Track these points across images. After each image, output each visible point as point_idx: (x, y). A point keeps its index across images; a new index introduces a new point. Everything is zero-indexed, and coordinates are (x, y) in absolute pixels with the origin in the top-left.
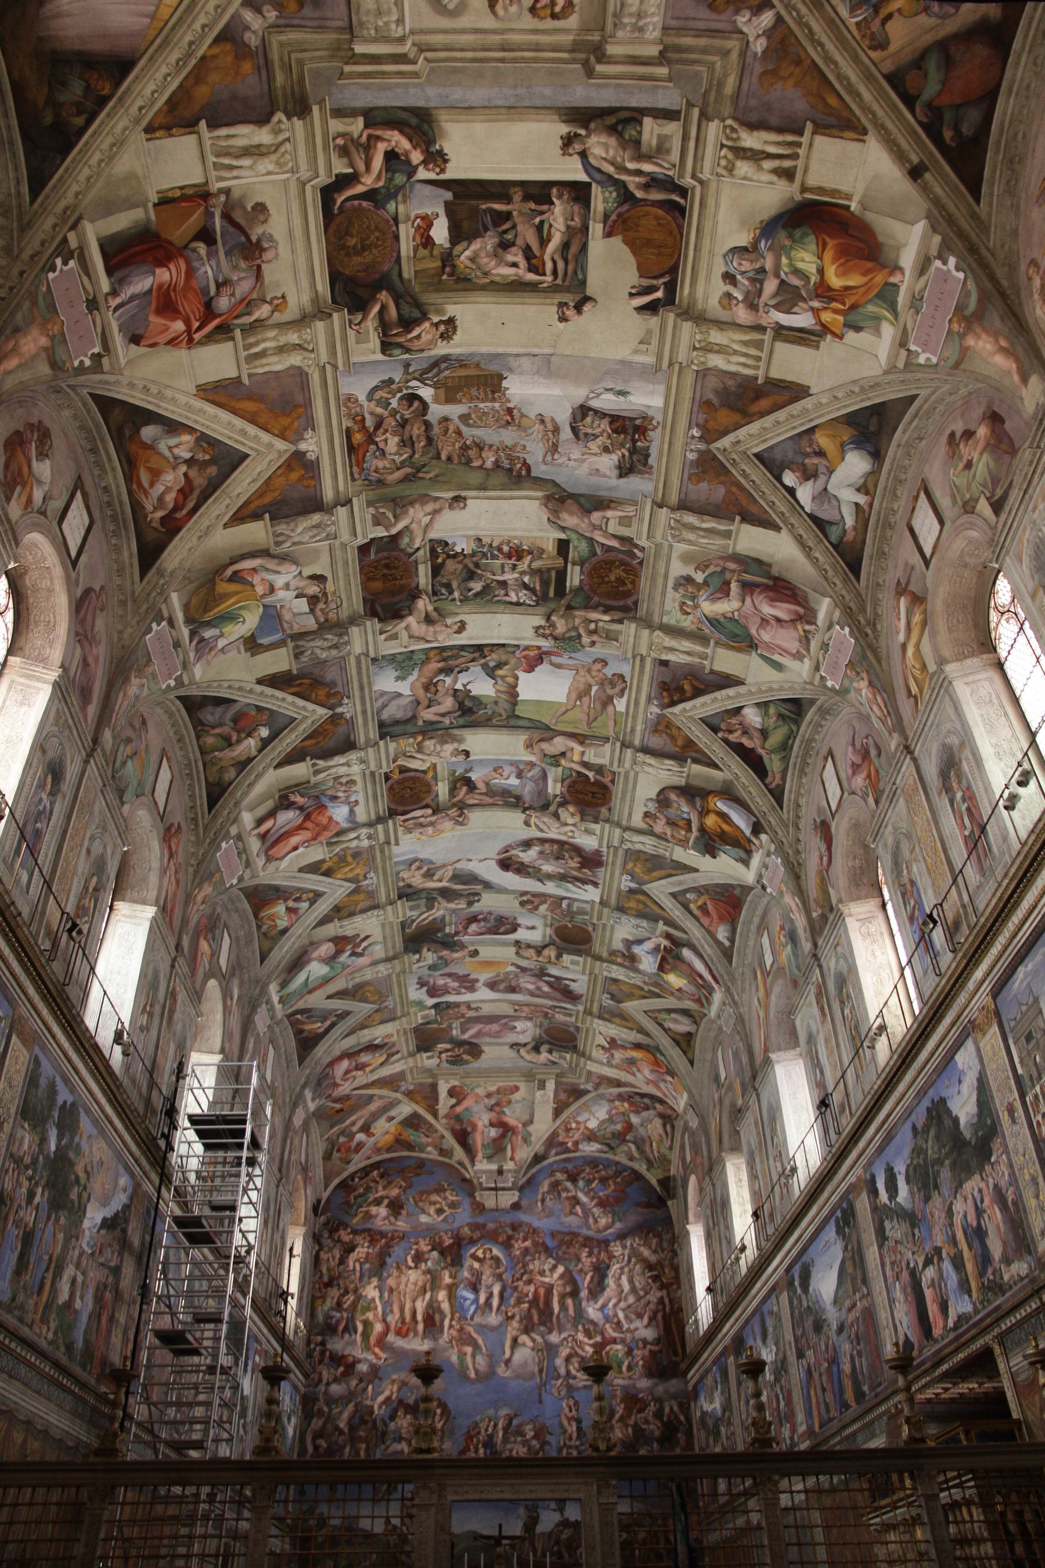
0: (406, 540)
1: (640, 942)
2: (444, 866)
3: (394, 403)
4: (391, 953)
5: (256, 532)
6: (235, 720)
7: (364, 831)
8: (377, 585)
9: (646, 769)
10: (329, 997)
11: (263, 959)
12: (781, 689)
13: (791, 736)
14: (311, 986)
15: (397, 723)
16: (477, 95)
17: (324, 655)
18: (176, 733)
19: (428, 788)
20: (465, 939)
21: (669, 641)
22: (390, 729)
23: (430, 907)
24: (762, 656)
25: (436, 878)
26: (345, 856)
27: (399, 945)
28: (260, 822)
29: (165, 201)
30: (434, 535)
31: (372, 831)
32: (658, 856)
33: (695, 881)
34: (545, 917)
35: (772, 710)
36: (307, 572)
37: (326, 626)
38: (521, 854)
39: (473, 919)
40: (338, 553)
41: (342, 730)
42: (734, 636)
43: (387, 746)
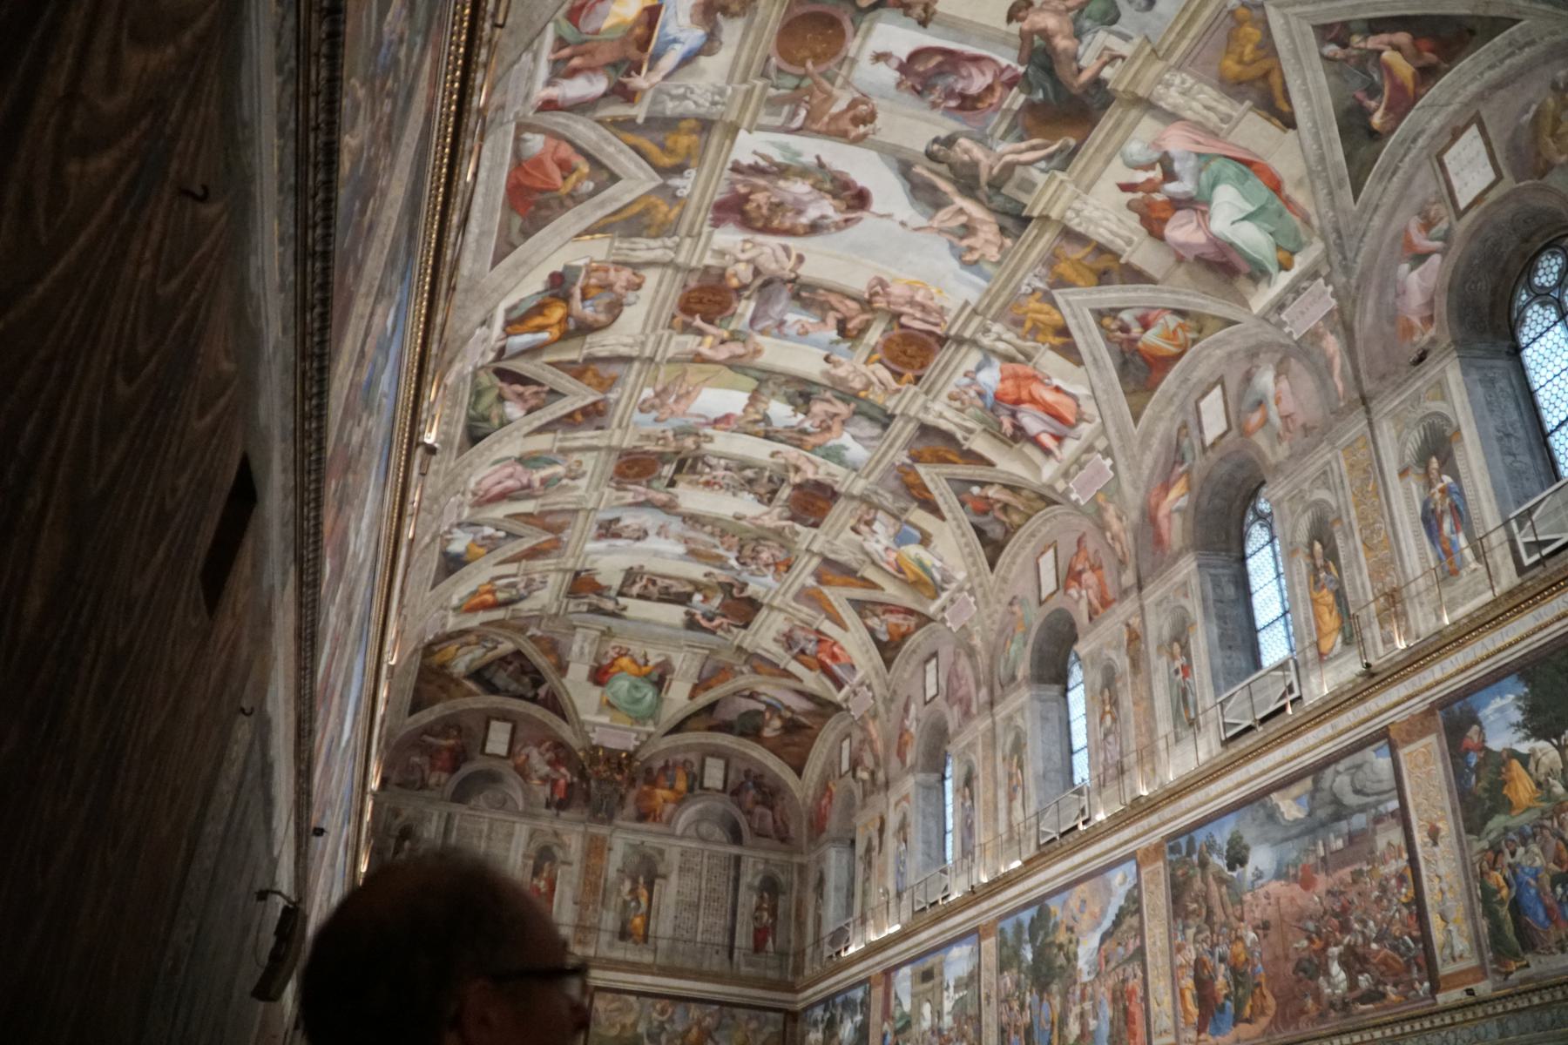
0: (787, 514)
1: (687, 60)
2: (941, 231)
3: (754, 567)
4: (1134, 113)
5: (870, 573)
6: (985, 513)
7: (986, 341)
8: (821, 504)
9: (630, 341)
10: (1289, 122)
11: (1230, 323)
12: (489, 448)
13: (473, 405)
14: (1265, 193)
15: (871, 419)
16: (659, 630)
17: (888, 495)
18: (1029, 542)
19: (887, 345)
20: (1007, 59)
21: (595, 442)
22: (881, 417)
23: (1009, 168)
24: (508, 458)
25: (963, 219)
26: (1030, 331)
27: (1107, 122)
28: (1047, 452)
29: (810, 669)
30: (765, 509)
31: (979, 336)
32: (630, 236)
33: (581, 217)
34: (847, 83)
35: (496, 422)
36: (858, 538)
37: (877, 507)
38: (830, 212)
39: (967, 103)
40: (833, 533)
41: (919, 446)
42: (536, 459)
43: (896, 407)
